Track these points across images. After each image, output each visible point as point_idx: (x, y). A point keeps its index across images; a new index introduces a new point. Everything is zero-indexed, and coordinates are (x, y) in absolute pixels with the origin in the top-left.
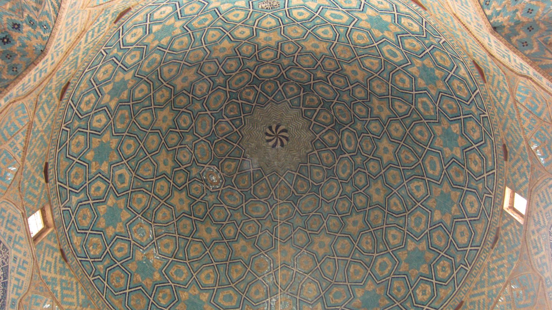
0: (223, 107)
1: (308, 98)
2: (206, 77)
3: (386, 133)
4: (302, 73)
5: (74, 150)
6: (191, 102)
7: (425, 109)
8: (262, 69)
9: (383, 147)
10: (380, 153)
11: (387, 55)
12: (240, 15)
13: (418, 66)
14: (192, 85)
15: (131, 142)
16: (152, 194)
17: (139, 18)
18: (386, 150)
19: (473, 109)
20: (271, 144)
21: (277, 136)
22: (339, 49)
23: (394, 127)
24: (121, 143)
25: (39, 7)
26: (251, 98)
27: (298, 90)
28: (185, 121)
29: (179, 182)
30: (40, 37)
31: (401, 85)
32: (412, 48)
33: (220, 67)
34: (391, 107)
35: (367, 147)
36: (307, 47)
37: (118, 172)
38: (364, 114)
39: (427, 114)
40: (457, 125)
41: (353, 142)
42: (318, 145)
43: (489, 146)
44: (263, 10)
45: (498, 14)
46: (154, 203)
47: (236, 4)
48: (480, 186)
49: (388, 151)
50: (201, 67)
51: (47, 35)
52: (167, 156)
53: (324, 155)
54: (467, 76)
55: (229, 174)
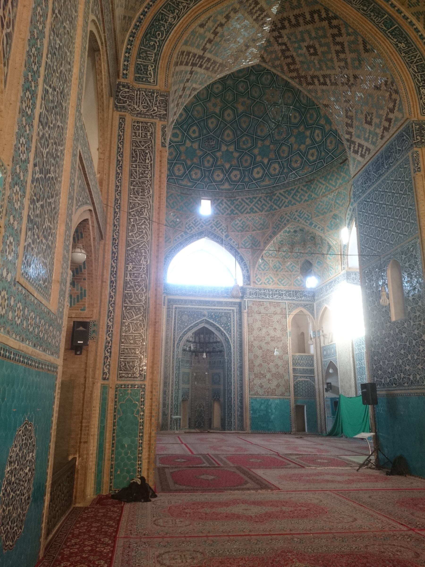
2: (261, 86)
33: (249, 89)
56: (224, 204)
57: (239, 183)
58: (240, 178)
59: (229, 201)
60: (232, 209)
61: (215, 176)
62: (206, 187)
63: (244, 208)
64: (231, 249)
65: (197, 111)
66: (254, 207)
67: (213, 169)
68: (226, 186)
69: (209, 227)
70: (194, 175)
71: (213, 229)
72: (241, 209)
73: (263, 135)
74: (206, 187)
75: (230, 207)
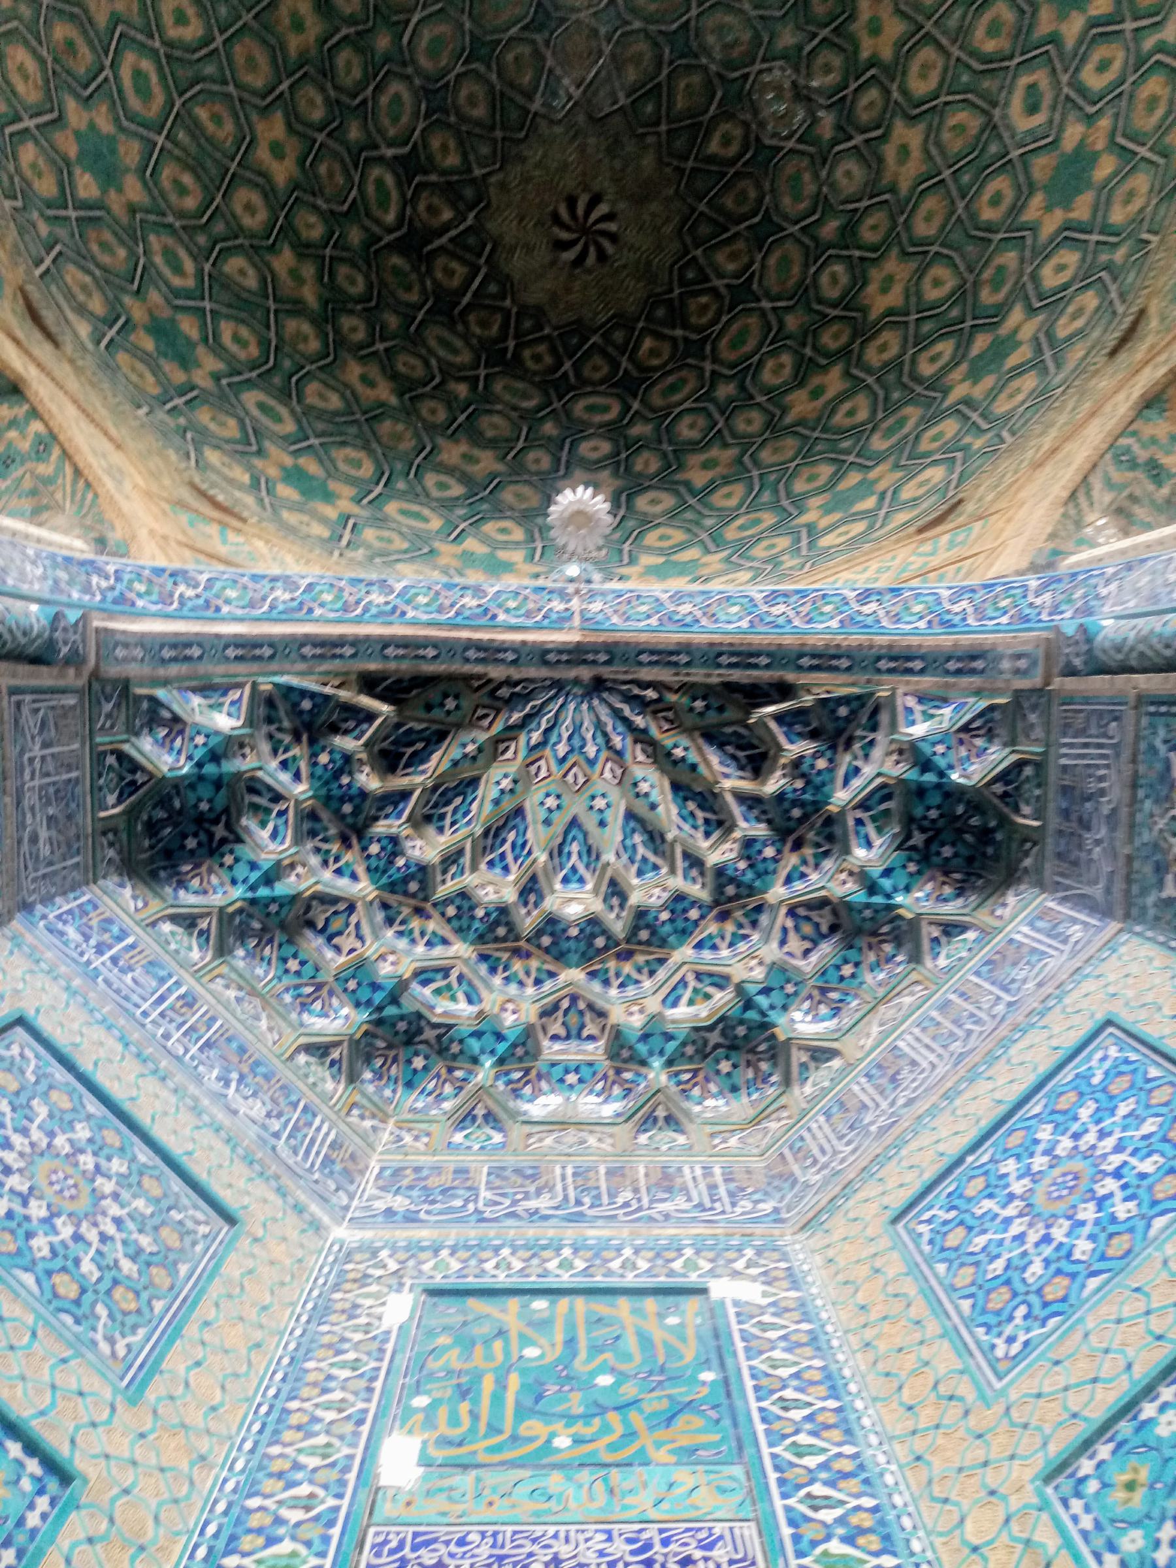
0: (724, 319)
1: (495, 330)
3: (283, 204)
4: (507, 397)
5: (1141, 182)
6: (809, 333)
7: (176, 255)
10: (293, 148)
11: (283, 411)
14: (799, 379)
15: (988, 214)
16: (956, 52)
17: (902, 517)
18: (277, 150)
19: (44, 229)
20: (603, 209)
21: (585, 231)
22: (408, 445)
24: (1017, 209)
25: (1127, 504)
26: (648, 343)
28: (833, 280)
29: (873, 94)
30: (1145, 438)
31: (244, 332)
34: (268, 279)
37: (1039, 119)
38: (343, 270)
40: (82, 194)
41: (370, 189)
42: (469, 193)
45: (13, 423)
46: (952, 22)
47: (661, 560)
51: (1124, 441)
52: (896, 174)
53: (452, 160)
55: (728, 116)
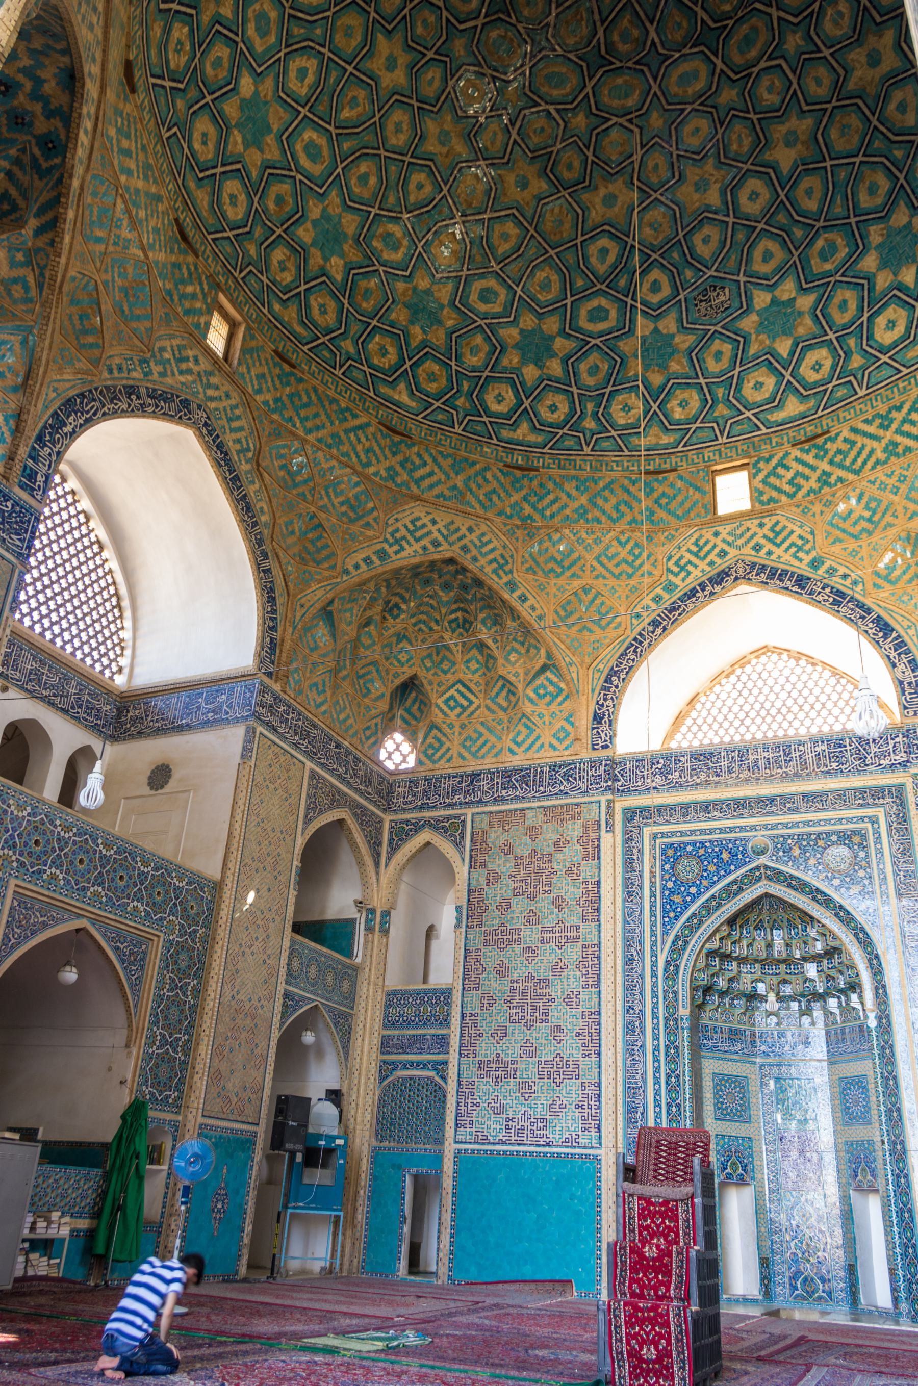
2: (826, 53)
4: (615, 103)
7: (389, 235)
8: (699, 85)
9: (400, 61)
12: (760, 259)
13: (445, 312)
14: (857, 37)
18: (391, 65)
23: (405, 127)
27: (613, 43)
32: (474, 343)
33: (795, 86)
35: (425, 21)
36: (624, 190)
39: (381, 230)
43: (299, 329)
44: (719, 284)
45: (457, 572)
48: (253, 251)
49: (387, 69)
50: (837, 86)
54: (396, 397)
56: (794, 465)
57: (834, 383)
58: (834, 368)
59: (808, 452)
60: (824, 473)
61: (748, 391)
62: (722, 433)
63: (864, 455)
64: (836, 603)
65: (651, 225)
66: (899, 439)
67: (736, 372)
68: (793, 407)
69: (748, 550)
70: (679, 410)
71: (765, 550)
72: (854, 461)
73: (879, 201)
74: (722, 433)
75: (813, 468)
